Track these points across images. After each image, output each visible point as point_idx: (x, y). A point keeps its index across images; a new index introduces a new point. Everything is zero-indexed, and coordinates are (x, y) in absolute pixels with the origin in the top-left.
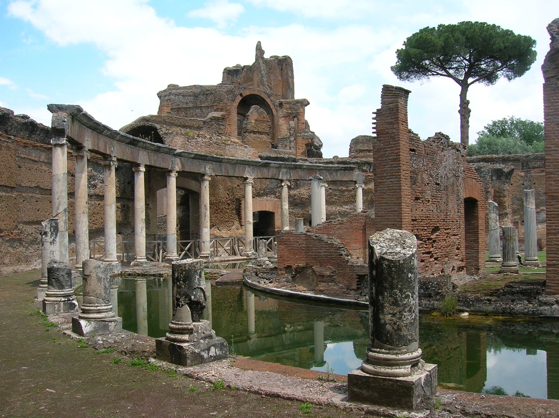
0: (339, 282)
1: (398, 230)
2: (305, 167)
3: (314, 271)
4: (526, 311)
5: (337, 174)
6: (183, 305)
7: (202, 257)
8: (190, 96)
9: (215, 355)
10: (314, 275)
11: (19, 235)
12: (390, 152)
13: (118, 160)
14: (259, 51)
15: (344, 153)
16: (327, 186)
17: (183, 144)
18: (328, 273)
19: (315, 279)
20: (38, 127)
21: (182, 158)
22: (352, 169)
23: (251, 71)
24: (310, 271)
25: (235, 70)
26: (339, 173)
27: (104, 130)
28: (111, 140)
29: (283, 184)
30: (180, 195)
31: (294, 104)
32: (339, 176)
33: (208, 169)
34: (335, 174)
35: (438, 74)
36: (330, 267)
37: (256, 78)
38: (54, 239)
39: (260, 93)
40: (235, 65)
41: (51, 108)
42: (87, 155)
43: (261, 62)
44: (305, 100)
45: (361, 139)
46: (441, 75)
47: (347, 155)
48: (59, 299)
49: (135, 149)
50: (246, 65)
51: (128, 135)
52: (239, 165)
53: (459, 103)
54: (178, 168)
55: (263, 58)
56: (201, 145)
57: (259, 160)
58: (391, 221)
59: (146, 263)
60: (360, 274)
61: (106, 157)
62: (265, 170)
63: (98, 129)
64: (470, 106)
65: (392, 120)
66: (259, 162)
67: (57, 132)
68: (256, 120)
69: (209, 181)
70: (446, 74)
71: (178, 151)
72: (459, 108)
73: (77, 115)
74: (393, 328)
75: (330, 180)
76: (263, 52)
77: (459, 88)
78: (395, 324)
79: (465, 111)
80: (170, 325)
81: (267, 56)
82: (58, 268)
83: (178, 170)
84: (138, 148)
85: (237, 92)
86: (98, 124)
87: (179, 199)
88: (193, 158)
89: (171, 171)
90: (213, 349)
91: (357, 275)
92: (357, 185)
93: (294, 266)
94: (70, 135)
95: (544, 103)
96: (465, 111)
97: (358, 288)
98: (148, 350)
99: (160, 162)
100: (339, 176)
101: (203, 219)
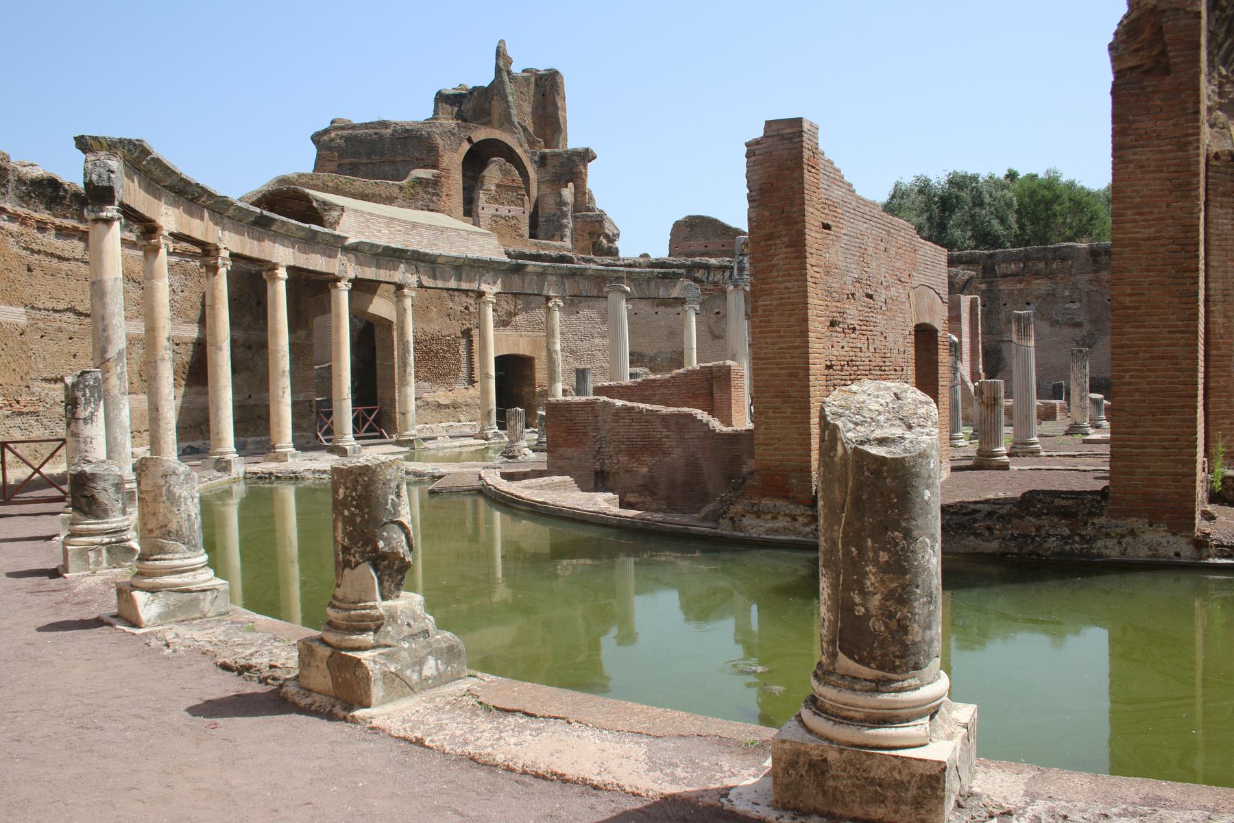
1: (889, 384)
2: (590, 272)
4: (1067, 548)
6: (357, 564)
7: (399, 443)
9: (435, 673)
11: (33, 404)
13: (234, 256)
15: (660, 250)
20: (66, 191)
22: (676, 277)
25: (456, 96)
27: (200, 196)
34: (645, 286)
37: (497, 108)
38: (92, 413)
39: (506, 136)
40: (456, 86)
41: (83, 144)
42: (165, 245)
43: (506, 78)
48: (97, 539)
50: (477, 85)
51: (252, 208)
54: (352, 274)
55: (509, 73)
57: (506, 259)
58: (786, 369)
61: (207, 251)
62: (516, 279)
63: (189, 195)
66: (505, 263)
67: (99, 194)
68: (498, 186)
71: (352, 240)
73: (139, 158)
74: (887, 626)
76: (509, 61)
78: (891, 616)
80: (330, 611)
81: (516, 69)
82: (92, 474)
86: (187, 183)
89: (338, 279)
90: (431, 662)
92: (687, 307)
94: (126, 201)
95: (1113, 123)
98: (282, 661)
99: (317, 262)
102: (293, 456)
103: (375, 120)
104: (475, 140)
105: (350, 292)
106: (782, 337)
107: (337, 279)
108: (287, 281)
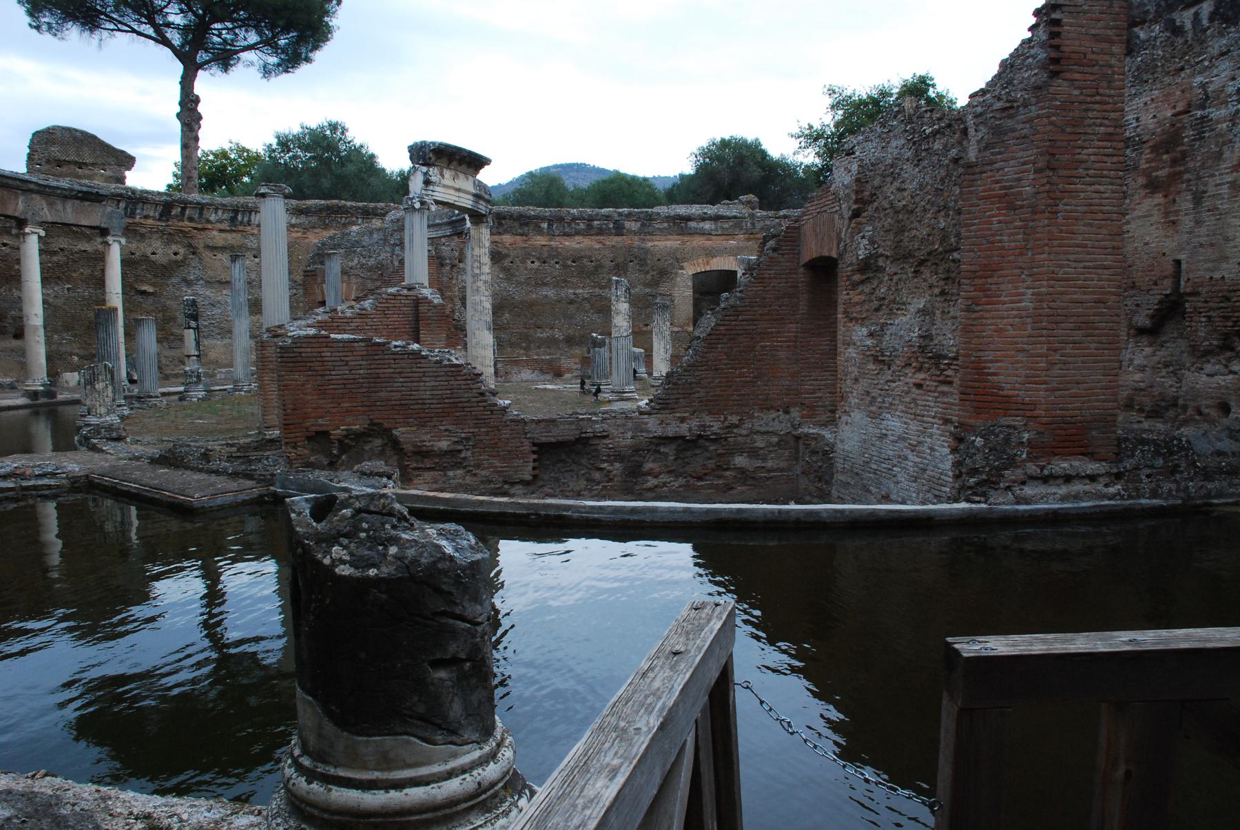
0: (478, 466)
3: (395, 444)
5: (64, 208)
12: (1099, 115)
16: (43, 233)
18: (444, 444)
24: (378, 442)
26: (69, 205)
32: (69, 213)
34: (60, 207)
36: (450, 427)
46: (139, 34)
47: (24, 170)
53: (178, 99)
60: (544, 439)
64: (200, 108)
65: (1109, 32)
72: (178, 109)
75: (50, 219)
77: (178, 68)
91: (534, 444)
92: (110, 239)
93: (337, 433)
97: (535, 477)
100: (69, 213)
106: (1089, 253)
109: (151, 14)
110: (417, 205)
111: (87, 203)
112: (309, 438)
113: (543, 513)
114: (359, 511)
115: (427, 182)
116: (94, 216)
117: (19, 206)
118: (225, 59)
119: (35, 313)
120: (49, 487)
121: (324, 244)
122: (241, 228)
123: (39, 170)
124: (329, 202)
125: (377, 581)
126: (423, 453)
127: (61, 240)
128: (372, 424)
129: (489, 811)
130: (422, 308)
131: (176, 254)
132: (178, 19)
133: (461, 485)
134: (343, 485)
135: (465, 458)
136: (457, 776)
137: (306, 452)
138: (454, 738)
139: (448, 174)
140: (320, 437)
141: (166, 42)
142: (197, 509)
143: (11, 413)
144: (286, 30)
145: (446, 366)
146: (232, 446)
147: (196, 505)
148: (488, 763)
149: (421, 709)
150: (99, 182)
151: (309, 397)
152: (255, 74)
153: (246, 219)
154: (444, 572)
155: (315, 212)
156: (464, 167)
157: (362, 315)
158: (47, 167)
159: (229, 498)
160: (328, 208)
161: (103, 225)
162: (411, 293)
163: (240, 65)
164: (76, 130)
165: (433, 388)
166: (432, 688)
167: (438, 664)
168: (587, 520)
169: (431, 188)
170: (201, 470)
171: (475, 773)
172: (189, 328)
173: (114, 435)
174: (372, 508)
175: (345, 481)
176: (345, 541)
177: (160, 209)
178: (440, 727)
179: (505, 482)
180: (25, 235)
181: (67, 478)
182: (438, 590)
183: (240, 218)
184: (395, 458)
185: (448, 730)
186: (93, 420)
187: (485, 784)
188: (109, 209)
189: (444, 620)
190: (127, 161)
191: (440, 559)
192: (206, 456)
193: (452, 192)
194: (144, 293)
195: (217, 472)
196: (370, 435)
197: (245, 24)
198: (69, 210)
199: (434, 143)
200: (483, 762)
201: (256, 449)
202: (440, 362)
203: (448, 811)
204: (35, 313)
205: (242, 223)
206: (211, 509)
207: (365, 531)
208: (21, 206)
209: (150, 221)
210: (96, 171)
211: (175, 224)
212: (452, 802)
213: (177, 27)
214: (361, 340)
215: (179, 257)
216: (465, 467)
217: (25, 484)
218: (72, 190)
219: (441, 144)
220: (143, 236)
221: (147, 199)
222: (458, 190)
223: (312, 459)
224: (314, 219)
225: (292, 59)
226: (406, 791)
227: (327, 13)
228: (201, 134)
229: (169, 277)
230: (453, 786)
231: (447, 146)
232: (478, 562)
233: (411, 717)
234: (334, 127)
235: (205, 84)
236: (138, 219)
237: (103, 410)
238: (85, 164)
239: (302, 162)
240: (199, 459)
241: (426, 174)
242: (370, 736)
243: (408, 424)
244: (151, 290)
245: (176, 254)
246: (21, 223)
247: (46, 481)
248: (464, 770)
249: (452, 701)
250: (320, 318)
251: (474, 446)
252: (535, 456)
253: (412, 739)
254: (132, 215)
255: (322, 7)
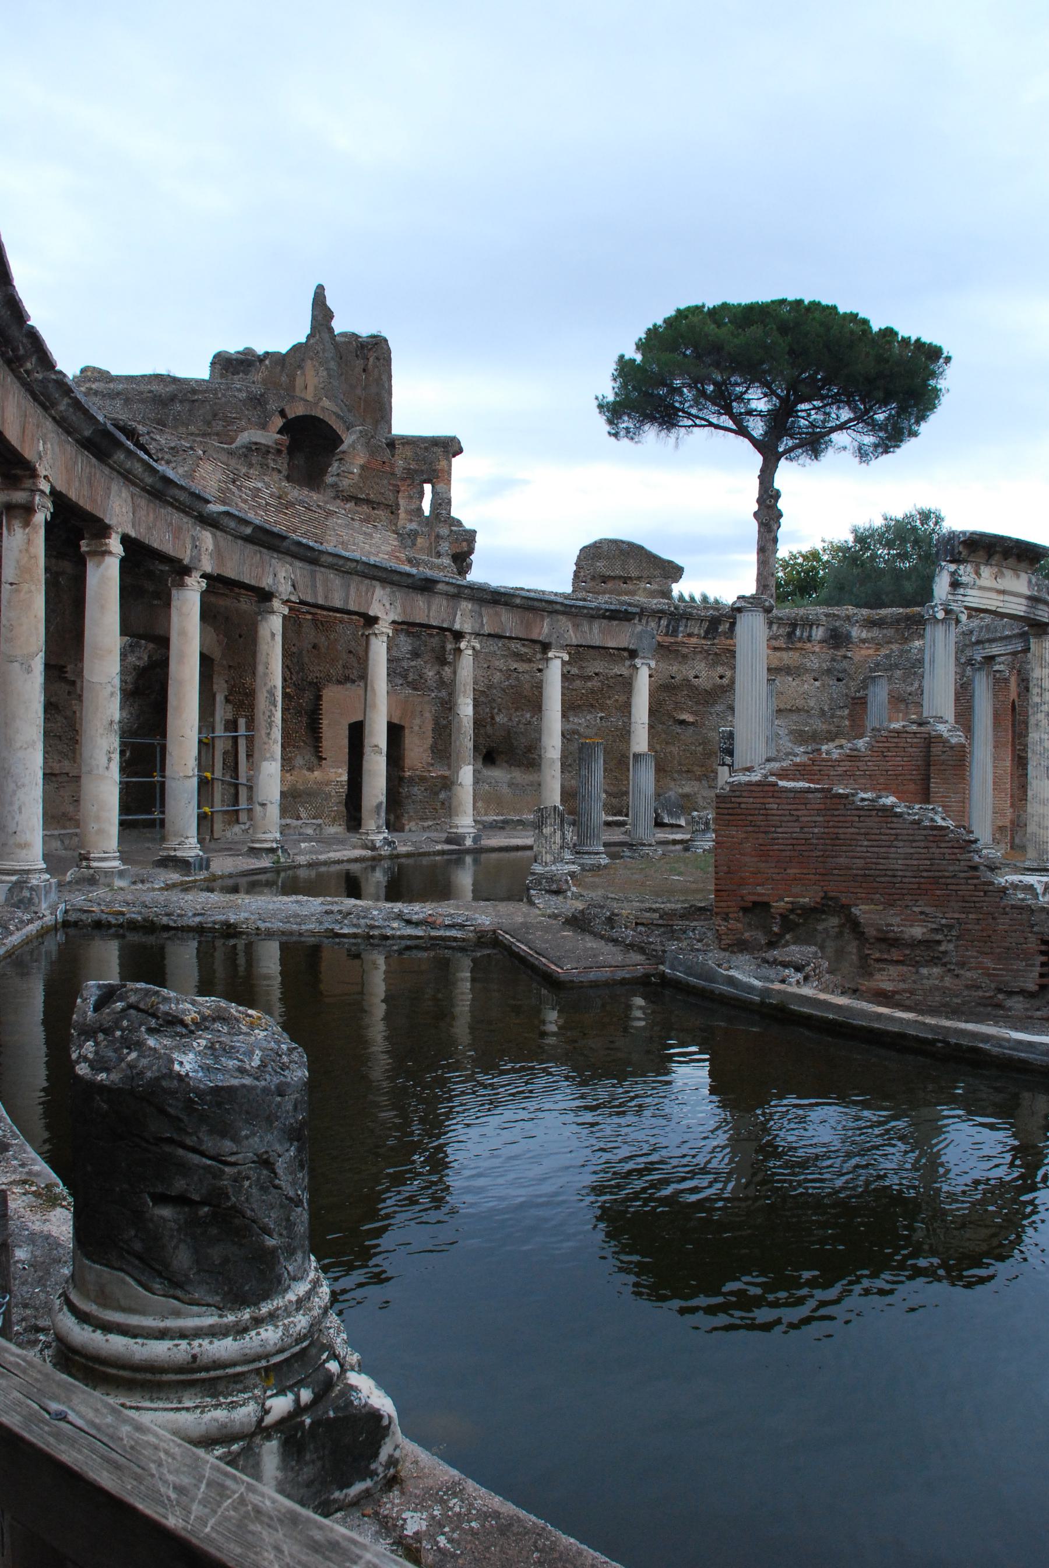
0: (962, 965)
2: (518, 601)
3: (854, 925)
5: (591, 629)
7: (254, 852)
8: (143, 401)
10: (847, 935)
13: (56, 496)
14: (321, 312)
15: (559, 582)
16: (566, 658)
17: (221, 490)
18: (918, 932)
19: (852, 948)
21: (219, 533)
23: (283, 366)
24: (834, 921)
25: (241, 362)
26: (596, 626)
28: (39, 410)
29: (463, 645)
30: (136, 668)
31: (426, 448)
32: (595, 634)
33: (281, 577)
34: (586, 628)
35: (711, 424)
36: (927, 910)
40: (241, 349)
44: (455, 438)
45: (605, 548)
46: (717, 427)
47: (568, 589)
49: (101, 473)
52: (356, 578)
53: (756, 495)
55: (331, 330)
56: (267, 504)
59: (121, 874)
64: (780, 505)
68: (363, 467)
69: (284, 617)
70: (734, 427)
71: (215, 508)
72: (756, 507)
75: (575, 642)
76: (329, 315)
77: (758, 460)
79: (768, 512)
81: (339, 326)
83: (208, 569)
84: (107, 471)
85: (273, 406)
87: (129, 679)
88: (248, 539)
92: (638, 662)
93: (779, 906)
96: (768, 512)
97: (1042, 987)
100: (595, 634)
101: (263, 732)
102: (121, 874)
103: (148, 371)
104: (291, 415)
105: (203, 594)
107: (183, 571)
108: (123, 561)
109: (724, 401)
110: (940, 615)
111: (615, 623)
112: (745, 910)
113: (953, 1041)
114: (131, 1006)
115: (955, 585)
116: (621, 637)
117: (543, 629)
118: (814, 444)
119: (553, 745)
120: (455, 939)
121: (877, 665)
122: (799, 645)
123: (584, 588)
124: (908, 610)
125: (101, 1088)
126: (889, 941)
127: (596, 663)
128: (825, 897)
129: (213, 1396)
130: (936, 750)
131: (721, 677)
132: (760, 403)
133: (937, 988)
134: (732, 973)
135: (945, 953)
136: (172, 1339)
137: (739, 925)
138: (179, 1293)
139: (986, 572)
140: (758, 908)
141: (742, 431)
142: (564, 982)
143: (520, 854)
144: (884, 402)
145: (926, 828)
146: (655, 911)
147: (563, 977)
148: (225, 1335)
149: (138, 1246)
150: (642, 597)
151: (747, 859)
152: (849, 458)
153: (805, 634)
154: (172, 1093)
155: (892, 624)
156: (1011, 561)
157: (853, 757)
158: (592, 584)
159: (605, 974)
160: (908, 617)
161: (631, 647)
162: (922, 729)
163: (830, 450)
164: (623, 542)
165: (909, 856)
166: (151, 1225)
167: (162, 1199)
168: (1011, 1059)
169: (961, 591)
170: (602, 937)
171: (196, 1343)
172: (724, 764)
173: (554, 887)
174: (142, 1006)
175: (737, 968)
176: (101, 1036)
177: (706, 625)
178: (160, 1274)
179: (1000, 990)
180: (548, 660)
181: (474, 931)
182: (162, 1112)
183: (798, 633)
184: (855, 943)
185: (170, 1280)
186: (538, 868)
187: (204, 1360)
188: (639, 628)
189: (168, 1149)
190: (674, 572)
191: (164, 1077)
192: (610, 921)
193: (994, 595)
194: (682, 722)
195: (615, 941)
196: (823, 912)
197: (836, 400)
198: (596, 631)
199: (964, 533)
200: (214, 1333)
201: (682, 917)
202: (918, 822)
203: (149, 1376)
204: (553, 745)
205: (800, 639)
206: (581, 986)
207: (123, 1030)
208: (546, 630)
209: (694, 640)
210: (642, 585)
211: (721, 641)
212: (152, 1368)
213: (760, 414)
214: (817, 790)
215: (725, 681)
216: (944, 965)
217: (434, 933)
218: (598, 609)
219: (973, 533)
220: (685, 657)
221: (691, 614)
222: (1003, 592)
223: (747, 935)
224: (890, 632)
225: (892, 437)
226: (112, 1337)
227: (933, 375)
228: (780, 533)
229: (713, 705)
230: (159, 1350)
231: (983, 536)
232: (230, 1089)
233: (128, 1253)
234: (925, 516)
235: (789, 476)
236: (680, 638)
237: (549, 858)
238: (630, 578)
239: (885, 562)
240: (604, 923)
241: (953, 574)
242: (94, 1262)
243: (872, 902)
244: (690, 718)
245: (721, 677)
246: (546, 647)
247: (453, 933)
248: (183, 1335)
249: (176, 1247)
250: (798, 760)
251: (958, 938)
252: (1044, 959)
253: (128, 1279)
254: (675, 633)
255: (927, 367)
